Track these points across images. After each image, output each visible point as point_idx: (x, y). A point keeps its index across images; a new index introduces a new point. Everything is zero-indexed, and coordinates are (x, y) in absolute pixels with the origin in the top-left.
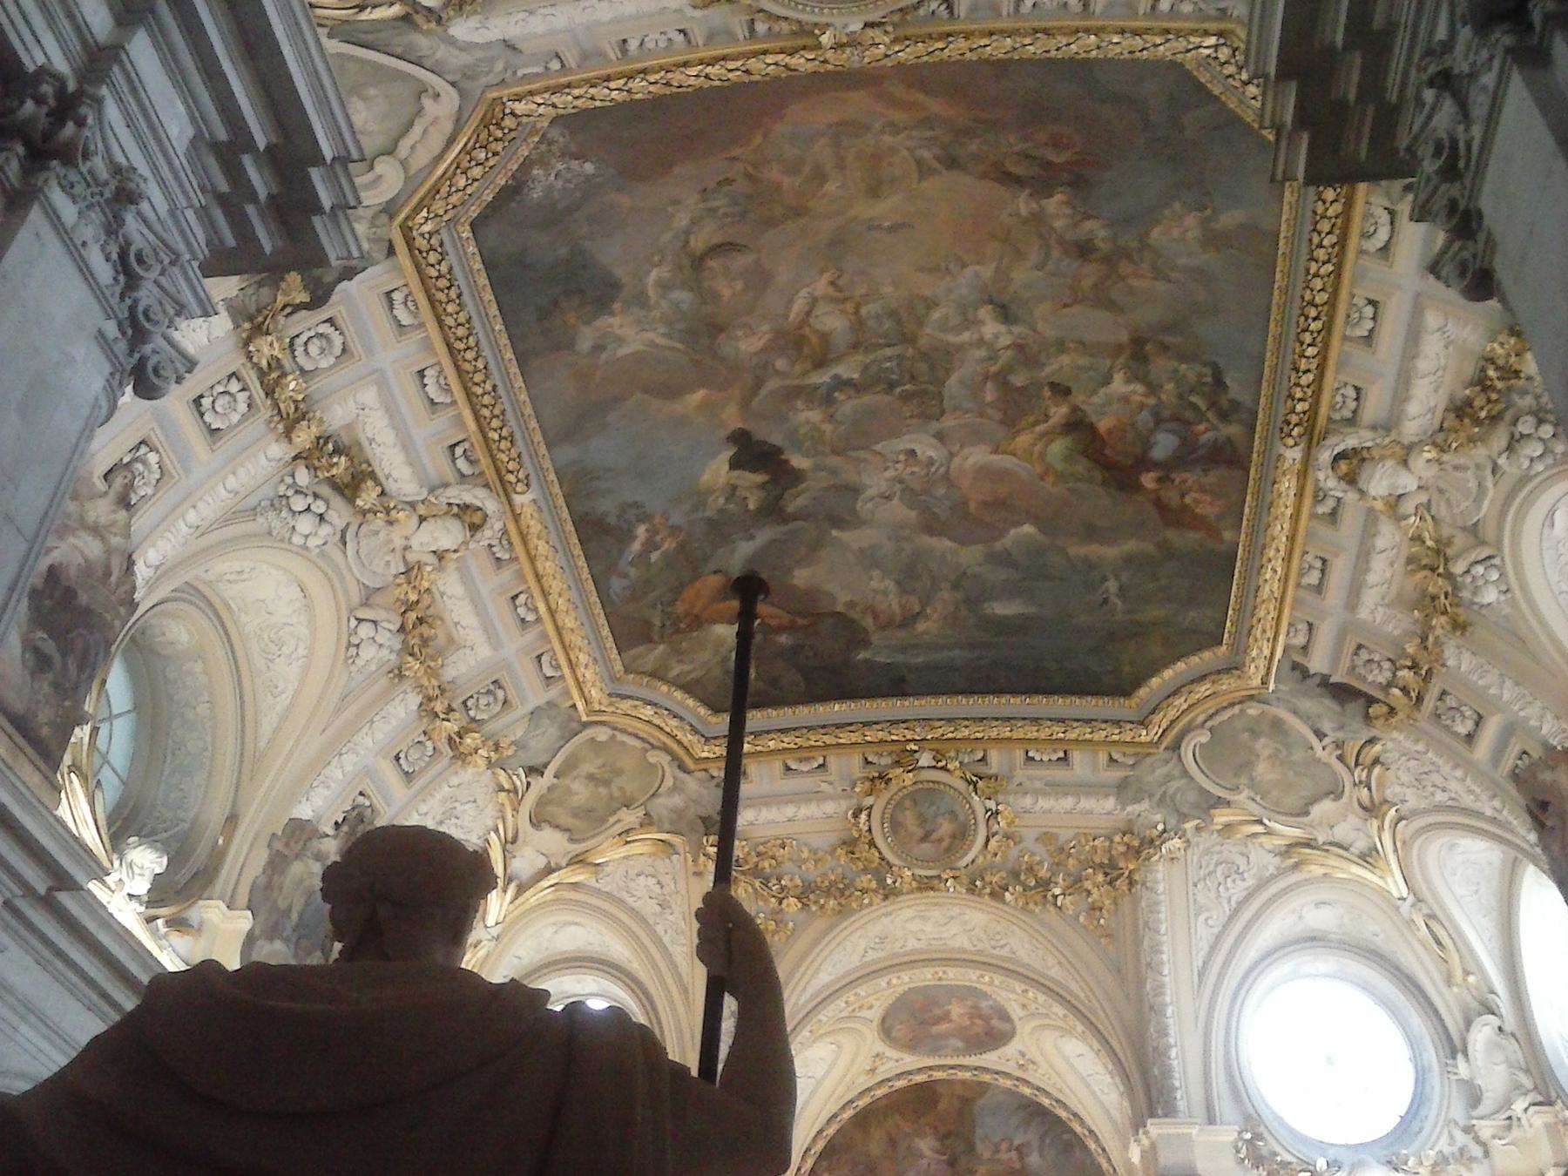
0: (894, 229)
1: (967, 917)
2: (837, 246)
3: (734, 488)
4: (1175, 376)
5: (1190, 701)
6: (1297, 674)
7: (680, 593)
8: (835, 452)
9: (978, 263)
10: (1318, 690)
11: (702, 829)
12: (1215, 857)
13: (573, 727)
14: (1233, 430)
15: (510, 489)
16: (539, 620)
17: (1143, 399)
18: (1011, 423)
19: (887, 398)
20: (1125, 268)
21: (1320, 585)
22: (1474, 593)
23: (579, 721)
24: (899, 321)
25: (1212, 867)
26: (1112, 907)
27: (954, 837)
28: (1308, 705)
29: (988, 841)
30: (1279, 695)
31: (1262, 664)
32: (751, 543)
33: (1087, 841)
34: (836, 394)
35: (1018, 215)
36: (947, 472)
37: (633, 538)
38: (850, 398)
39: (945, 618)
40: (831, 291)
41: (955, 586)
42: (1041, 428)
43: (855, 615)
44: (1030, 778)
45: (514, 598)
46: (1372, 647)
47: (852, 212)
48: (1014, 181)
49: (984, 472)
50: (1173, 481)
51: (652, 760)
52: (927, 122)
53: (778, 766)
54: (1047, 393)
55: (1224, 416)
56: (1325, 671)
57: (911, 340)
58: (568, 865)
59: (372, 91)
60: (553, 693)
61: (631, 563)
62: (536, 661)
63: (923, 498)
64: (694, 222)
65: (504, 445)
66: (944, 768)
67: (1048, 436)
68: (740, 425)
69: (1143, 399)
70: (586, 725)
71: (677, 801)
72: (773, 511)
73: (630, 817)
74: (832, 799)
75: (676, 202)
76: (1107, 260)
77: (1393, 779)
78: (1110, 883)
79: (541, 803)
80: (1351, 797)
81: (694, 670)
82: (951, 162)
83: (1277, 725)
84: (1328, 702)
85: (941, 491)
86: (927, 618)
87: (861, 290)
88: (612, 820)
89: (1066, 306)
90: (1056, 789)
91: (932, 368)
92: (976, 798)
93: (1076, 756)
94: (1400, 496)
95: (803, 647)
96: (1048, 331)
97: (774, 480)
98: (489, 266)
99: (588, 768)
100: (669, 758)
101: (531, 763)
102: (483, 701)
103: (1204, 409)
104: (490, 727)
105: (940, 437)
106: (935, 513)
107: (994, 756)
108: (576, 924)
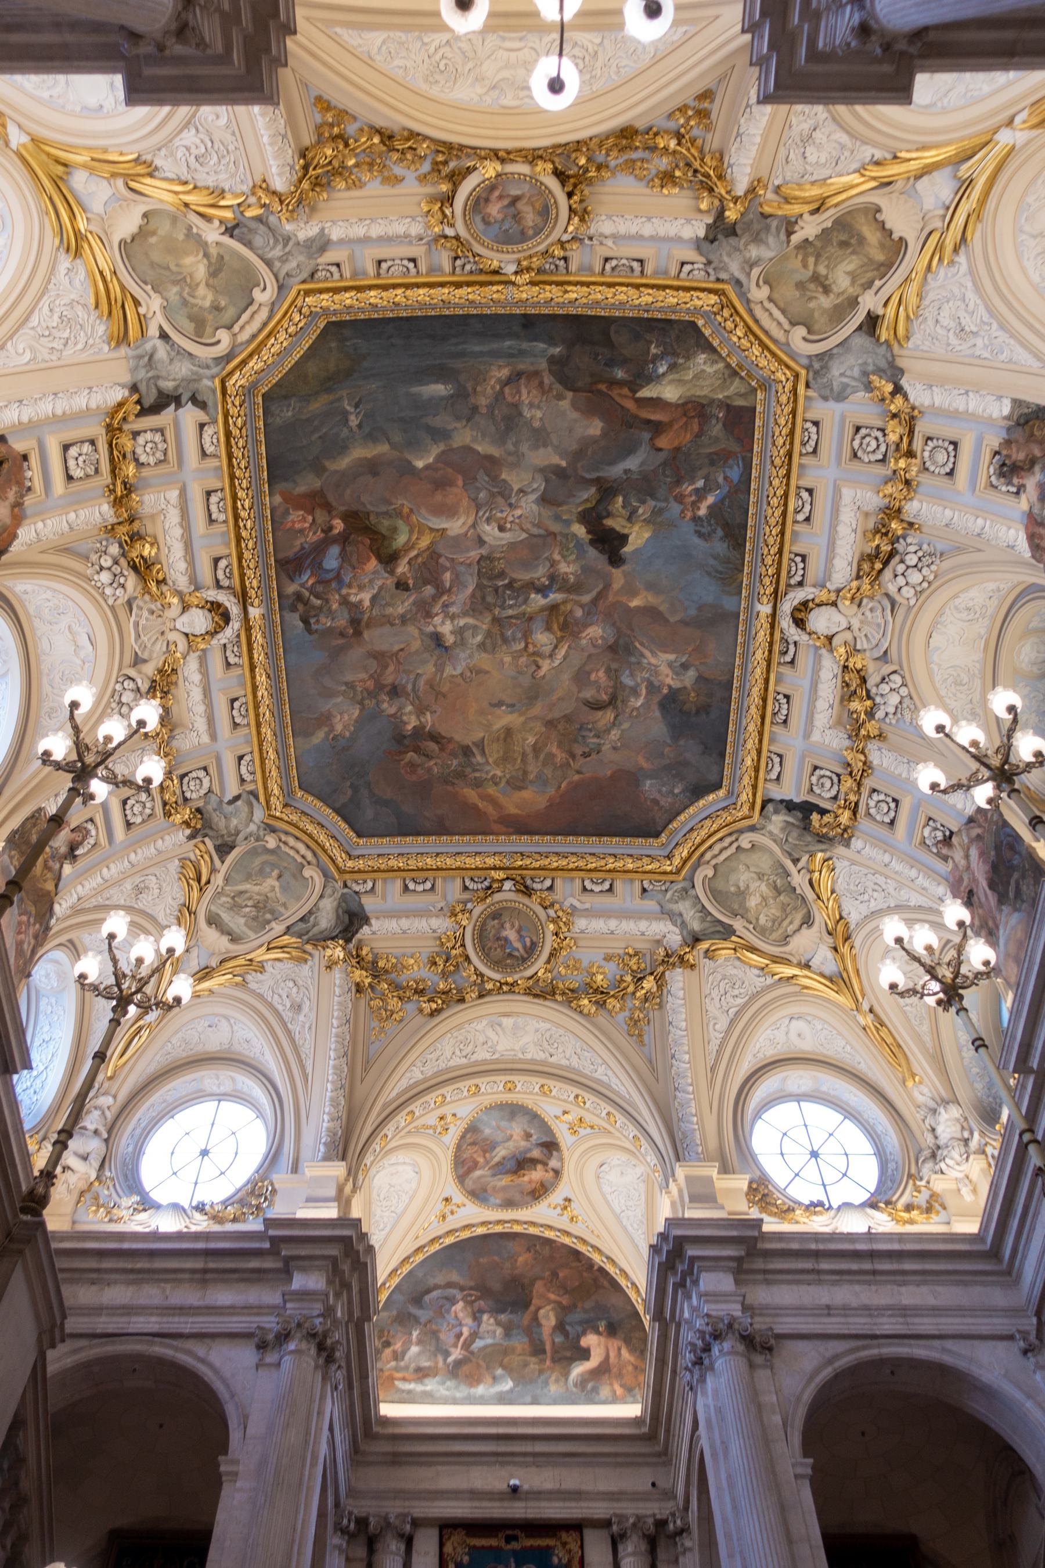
0: (500, 704)
2: (534, 693)
3: (629, 519)
4: (331, 613)
6: (200, 398)
8: (554, 535)
9: (453, 676)
10: (181, 390)
14: (291, 588)
16: (798, 488)
18: (433, 554)
19: (515, 576)
20: (370, 684)
24: (502, 635)
28: (183, 369)
35: (433, 712)
37: (709, 507)
40: (541, 662)
41: (475, 409)
47: (522, 719)
48: (435, 737)
49: (449, 511)
52: (478, 784)
54: (411, 582)
55: (299, 597)
56: (181, 411)
57: (496, 621)
59: (733, 889)
61: (718, 487)
64: (608, 731)
67: (408, 547)
68: (614, 570)
72: (607, 491)
73: (809, 228)
75: (615, 748)
76: (380, 687)
79: (885, 268)
82: (467, 751)
84: (168, 385)
85: (482, 495)
86: (499, 380)
87: (523, 660)
89: (402, 650)
91: (483, 598)
93: (371, 270)
94: (183, 612)
95: (606, 365)
96: (412, 630)
97: (600, 518)
98: (722, 755)
99: (826, 302)
105: (481, 542)
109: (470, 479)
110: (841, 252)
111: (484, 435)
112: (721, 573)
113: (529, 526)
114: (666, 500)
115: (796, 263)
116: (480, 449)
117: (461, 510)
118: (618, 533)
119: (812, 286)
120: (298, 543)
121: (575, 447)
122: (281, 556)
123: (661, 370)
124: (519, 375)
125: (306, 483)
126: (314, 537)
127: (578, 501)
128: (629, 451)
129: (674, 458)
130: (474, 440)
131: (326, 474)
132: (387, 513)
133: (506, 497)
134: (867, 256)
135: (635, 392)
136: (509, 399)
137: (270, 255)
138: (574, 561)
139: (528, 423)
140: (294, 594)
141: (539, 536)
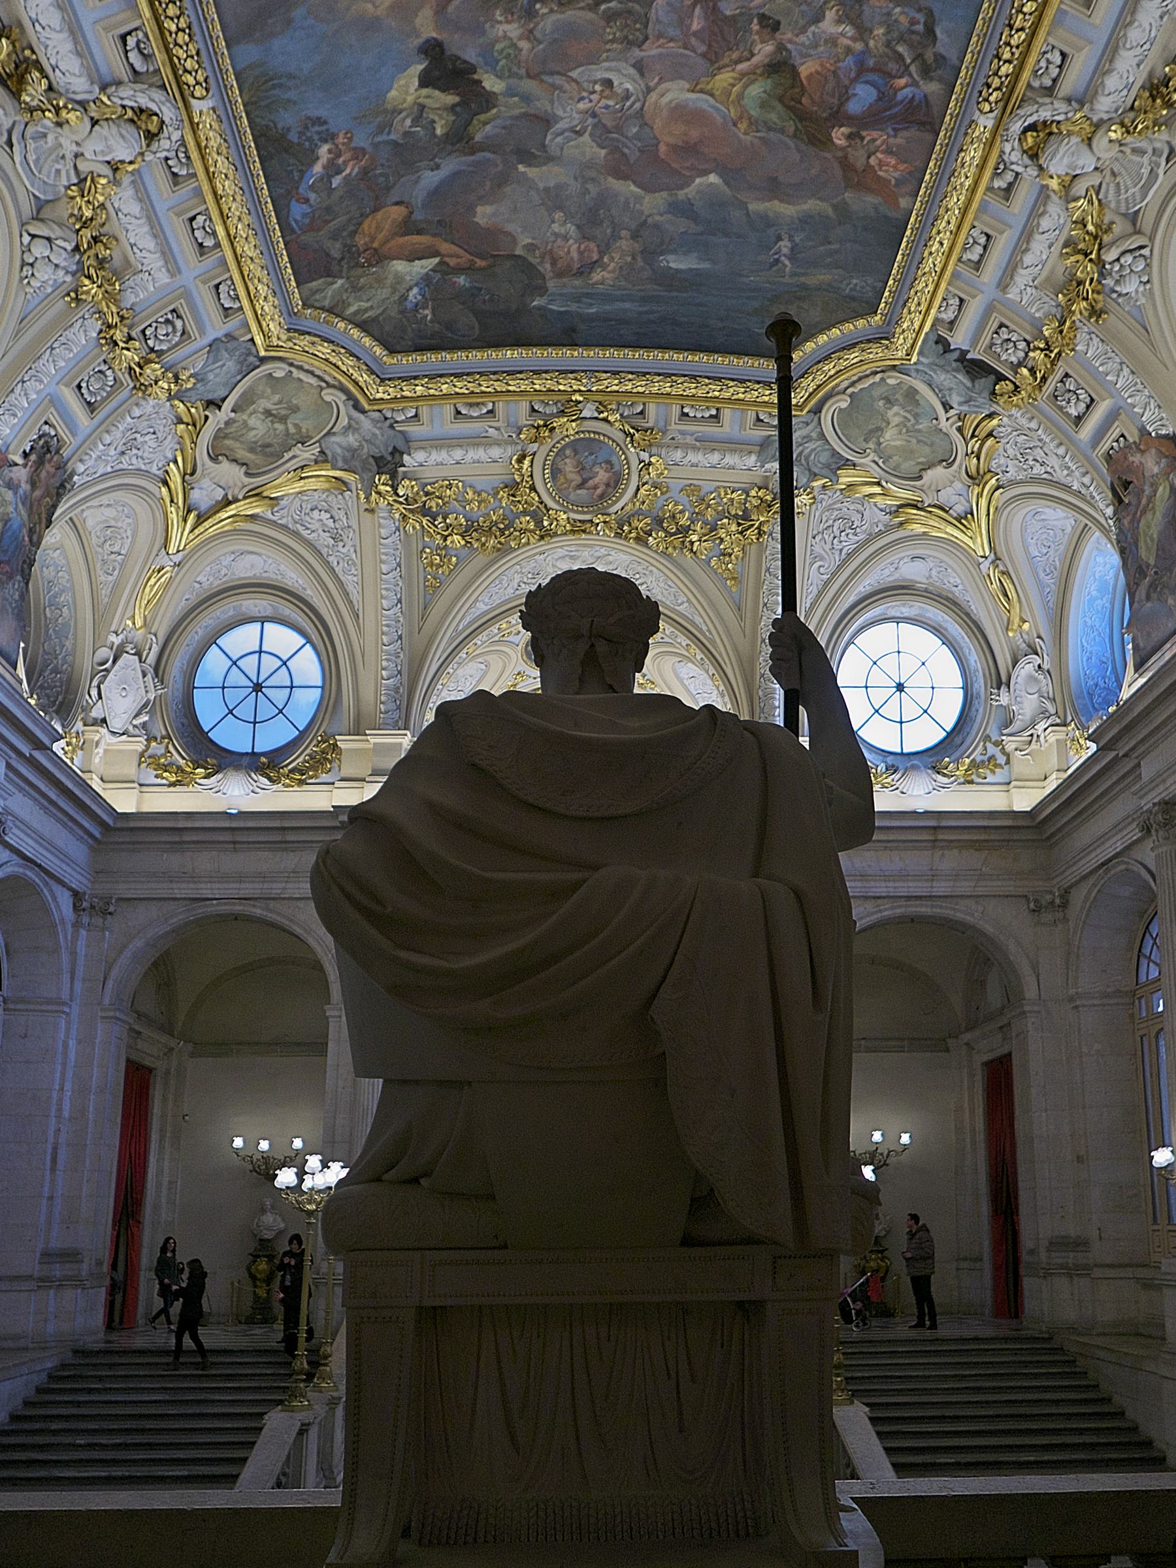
1: (611, 558)
3: (422, 107)
4: (890, 24)
5: (837, 368)
6: (940, 347)
7: (360, 224)
8: (529, 76)
11: (375, 468)
12: (836, 513)
13: (251, 361)
15: (187, 93)
16: (218, 245)
17: (849, 42)
18: (714, 59)
19: (590, 15)
21: (979, 262)
22: (1117, 282)
23: (257, 356)
25: (831, 522)
26: (740, 554)
27: (608, 485)
29: (638, 489)
30: (920, 367)
31: (911, 336)
32: (436, 172)
33: (726, 494)
34: (538, 6)
36: (642, 109)
37: (318, 158)
38: (552, 11)
39: (621, 268)
41: (635, 236)
42: (740, 67)
43: (534, 261)
44: (683, 433)
45: (193, 219)
46: (1012, 326)
49: (679, 112)
50: (862, 139)
51: (328, 398)
53: (448, 410)
54: (755, 26)
58: (245, 498)
60: (233, 323)
62: (213, 291)
63: (614, 135)
65: (182, 38)
66: (605, 420)
67: (749, 77)
68: (434, 35)
69: (849, 42)
70: (263, 360)
71: (352, 439)
72: (459, 139)
73: (306, 454)
74: (499, 445)
77: (1001, 450)
78: (741, 533)
79: (219, 436)
80: (961, 465)
81: (372, 307)
83: (912, 393)
86: (604, 267)
88: (287, 456)
90: (706, 444)
92: (632, 450)
93: (727, 414)
95: (480, 289)
99: (264, 404)
100: (344, 397)
101: (210, 397)
102: (162, 331)
103: (908, 61)
104: (168, 358)
105: (640, 67)
106: (624, 154)
107: (652, 409)
108: (252, 553)
109: (649, 151)
110: (268, 440)
111: (627, 202)
112: (274, 87)
113: (567, 87)
114: (376, 146)
115: (305, 426)
116: (633, 188)
117: (665, 113)
118: (436, 87)
119: (283, 412)
120: (899, 141)
121: (508, 189)
122: (929, 137)
123: (415, 290)
124: (580, 273)
125: (864, 203)
126: (876, 136)
127: (499, 121)
128: (436, 194)
129: (377, 198)
130: (639, 200)
131: (835, 201)
132: (770, 129)
133: (599, 125)
134: (242, 442)
135: (437, 264)
136: (592, 245)
137: (819, 443)
138: (497, 41)
139: (569, 216)
140: (931, 79)
141: (552, 74)
